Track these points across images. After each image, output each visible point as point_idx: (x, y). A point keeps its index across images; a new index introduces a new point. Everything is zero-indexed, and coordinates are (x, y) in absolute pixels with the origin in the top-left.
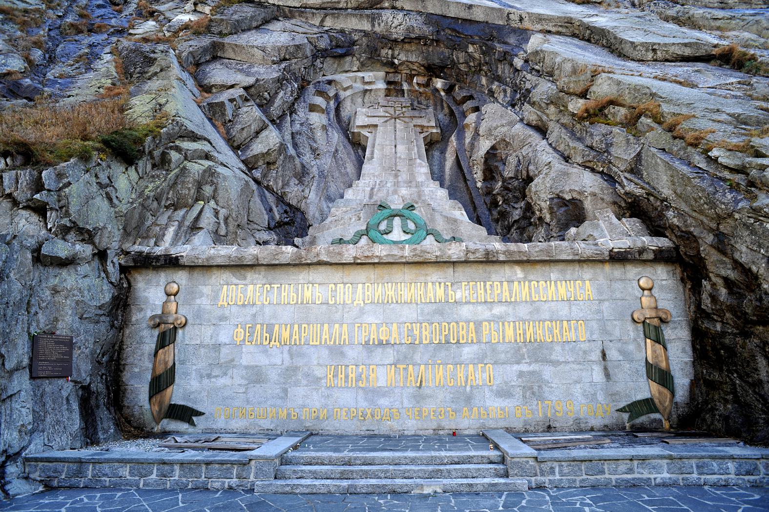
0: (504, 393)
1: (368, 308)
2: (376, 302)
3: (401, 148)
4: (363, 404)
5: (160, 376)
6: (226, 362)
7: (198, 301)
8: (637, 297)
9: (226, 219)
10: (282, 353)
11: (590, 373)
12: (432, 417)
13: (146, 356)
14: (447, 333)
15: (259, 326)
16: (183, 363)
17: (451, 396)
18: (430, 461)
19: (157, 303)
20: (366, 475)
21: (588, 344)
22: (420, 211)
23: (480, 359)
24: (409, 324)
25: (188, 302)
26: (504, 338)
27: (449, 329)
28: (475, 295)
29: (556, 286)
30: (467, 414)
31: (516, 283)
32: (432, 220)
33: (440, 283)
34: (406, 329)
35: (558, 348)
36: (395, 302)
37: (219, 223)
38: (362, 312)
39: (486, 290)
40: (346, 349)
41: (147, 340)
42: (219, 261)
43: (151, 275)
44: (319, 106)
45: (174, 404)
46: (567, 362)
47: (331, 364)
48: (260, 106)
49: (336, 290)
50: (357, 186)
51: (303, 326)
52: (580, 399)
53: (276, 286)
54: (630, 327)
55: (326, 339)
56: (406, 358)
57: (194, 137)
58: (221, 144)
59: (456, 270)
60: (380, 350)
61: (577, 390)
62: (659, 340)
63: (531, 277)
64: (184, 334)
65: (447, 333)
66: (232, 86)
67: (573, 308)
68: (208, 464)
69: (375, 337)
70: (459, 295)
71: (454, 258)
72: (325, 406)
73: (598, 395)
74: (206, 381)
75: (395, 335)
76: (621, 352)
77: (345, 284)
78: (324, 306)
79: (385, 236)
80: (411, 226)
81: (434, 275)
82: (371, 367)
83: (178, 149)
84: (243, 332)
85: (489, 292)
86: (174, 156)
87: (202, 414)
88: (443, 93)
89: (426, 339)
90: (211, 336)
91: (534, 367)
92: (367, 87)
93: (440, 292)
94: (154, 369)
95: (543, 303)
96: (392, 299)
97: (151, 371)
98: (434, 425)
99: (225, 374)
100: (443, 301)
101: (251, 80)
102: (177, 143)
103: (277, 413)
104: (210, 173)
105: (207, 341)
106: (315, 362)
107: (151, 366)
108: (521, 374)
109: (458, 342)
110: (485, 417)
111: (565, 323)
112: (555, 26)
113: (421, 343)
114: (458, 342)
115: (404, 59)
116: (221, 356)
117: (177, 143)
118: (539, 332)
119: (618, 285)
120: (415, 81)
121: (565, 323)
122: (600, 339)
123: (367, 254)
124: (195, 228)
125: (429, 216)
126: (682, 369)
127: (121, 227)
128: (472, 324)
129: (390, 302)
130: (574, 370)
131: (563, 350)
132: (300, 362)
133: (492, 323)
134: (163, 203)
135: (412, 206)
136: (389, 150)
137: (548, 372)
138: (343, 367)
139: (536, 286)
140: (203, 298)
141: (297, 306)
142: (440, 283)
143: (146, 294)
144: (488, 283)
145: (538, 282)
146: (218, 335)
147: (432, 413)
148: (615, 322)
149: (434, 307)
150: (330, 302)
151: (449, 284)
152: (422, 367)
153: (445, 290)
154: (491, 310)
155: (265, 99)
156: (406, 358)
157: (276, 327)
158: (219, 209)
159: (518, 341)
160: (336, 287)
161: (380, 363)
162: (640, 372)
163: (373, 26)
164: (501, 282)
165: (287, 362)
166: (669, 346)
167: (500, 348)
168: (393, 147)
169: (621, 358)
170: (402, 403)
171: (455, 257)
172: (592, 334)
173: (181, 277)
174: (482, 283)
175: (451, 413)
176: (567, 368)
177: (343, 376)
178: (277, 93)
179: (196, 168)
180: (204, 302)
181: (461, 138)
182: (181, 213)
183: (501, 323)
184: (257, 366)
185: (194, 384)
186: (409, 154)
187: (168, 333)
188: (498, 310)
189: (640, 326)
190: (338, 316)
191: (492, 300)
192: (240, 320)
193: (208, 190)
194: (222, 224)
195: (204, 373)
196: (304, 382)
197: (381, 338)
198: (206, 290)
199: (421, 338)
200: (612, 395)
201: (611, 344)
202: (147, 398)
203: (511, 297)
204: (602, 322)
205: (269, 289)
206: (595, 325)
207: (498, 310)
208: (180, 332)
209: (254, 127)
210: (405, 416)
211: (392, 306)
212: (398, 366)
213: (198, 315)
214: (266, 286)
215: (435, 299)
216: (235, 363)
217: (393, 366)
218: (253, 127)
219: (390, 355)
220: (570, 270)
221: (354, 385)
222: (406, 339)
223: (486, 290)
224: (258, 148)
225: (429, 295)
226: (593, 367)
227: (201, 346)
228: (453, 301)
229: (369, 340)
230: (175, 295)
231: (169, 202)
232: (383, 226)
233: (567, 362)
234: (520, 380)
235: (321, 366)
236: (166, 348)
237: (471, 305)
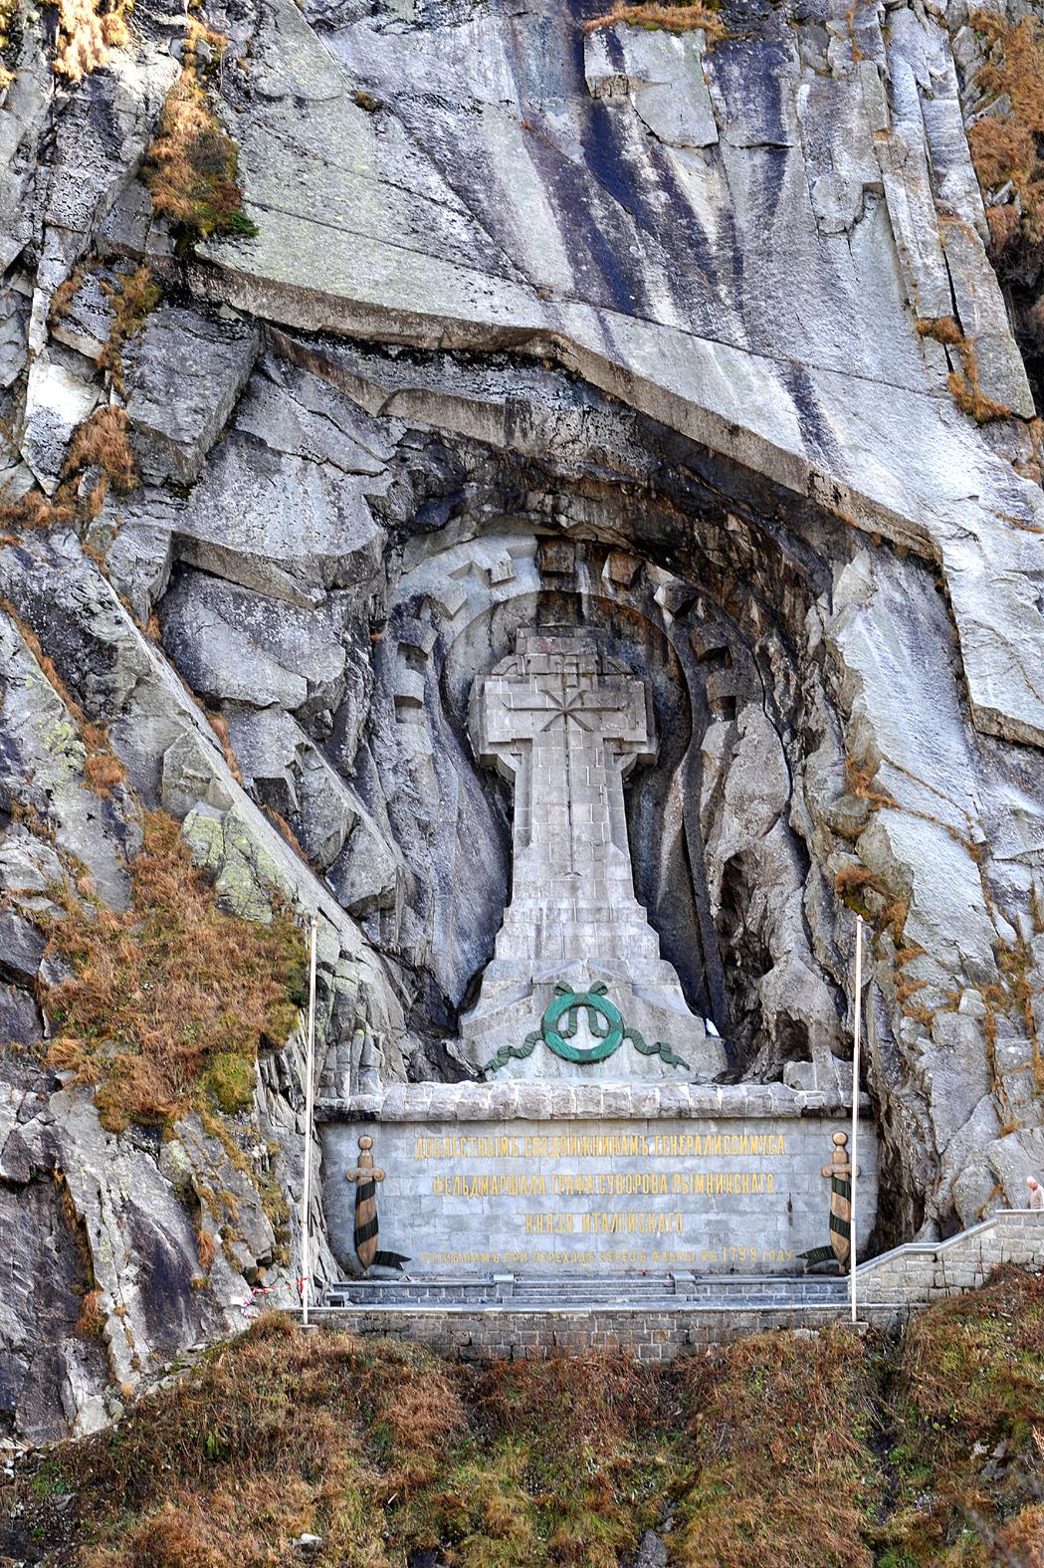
0: (692, 1239)
3: (580, 811)
4: (560, 1249)
7: (394, 1155)
16: (385, 1213)
18: (622, 1285)
20: (577, 1293)
22: (614, 996)
23: (671, 1209)
32: (632, 1012)
35: (746, 1200)
40: (543, 1199)
42: (417, 1118)
43: (341, 1129)
44: (413, 698)
46: (753, 1213)
50: (512, 922)
54: (819, 1181)
61: (761, 1238)
63: (725, 1132)
68: (465, 1287)
70: (652, 1148)
71: (648, 1116)
72: (525, 1251)
74: (409, 1229)
79: (567, 1041)
80: (602, 1023)
81: (629, 1130)
87: (408, 1260)
88: (668, 617)
91: (722, 1216)
92: (499, 595)
93: (634, 1146)
94: (356, 1220)
98: (626, 1267)
105: (407, 1192)
108: (709, 1223)
112: (900, 533)
115: (582, 517)
118: (730, 1186)
119: (812, 1140)
120: (606, 573)
132: (500, 1211)
135: (604, 987)
136: (558, 815)
137: (734, 1221)
163: (510, 433)
165: (487, 1212)
167: (691, 1198)
168: (566, 809)
172: (780, 1186)
173: (373, 1133)
176: (754, 1218)
180: (400, 1156)
181: (693, 782)
185: (398, 1233)
186: (595, 830)
188: (689, 1163)
189: (830, 1181)
190: (535, 1168)
196: (505, 1230)
198: (401, 1143)
204: (792, 1176)
206: (784, 1178)
207: (689, 1163)
213: (395, 1167)
219: (585, 1205)
220: (763, 1125)
227: (402, 1197)
232: (563, 1026)
233: (753, 1213)
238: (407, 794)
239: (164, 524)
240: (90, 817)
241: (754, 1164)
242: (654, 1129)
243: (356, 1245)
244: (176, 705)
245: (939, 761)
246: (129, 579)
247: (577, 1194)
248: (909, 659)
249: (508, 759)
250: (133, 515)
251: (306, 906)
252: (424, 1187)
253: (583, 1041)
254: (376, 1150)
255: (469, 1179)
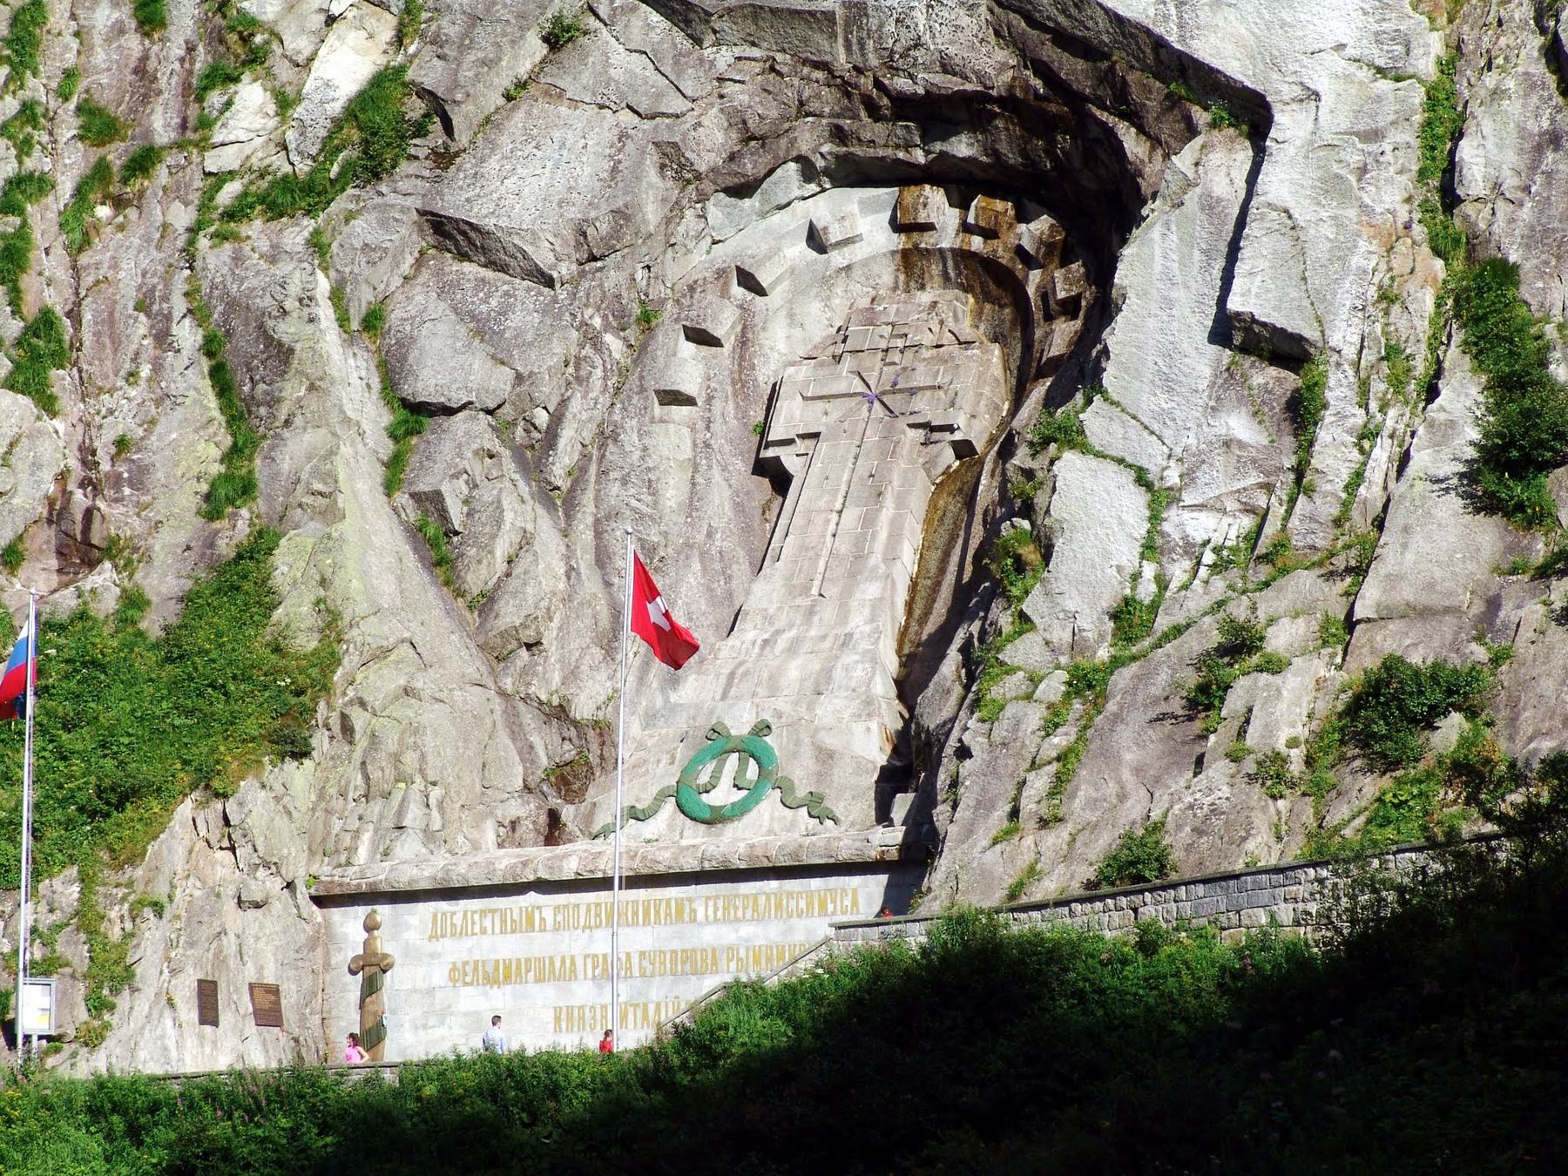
5: (370, 1029)
7: (405, 935)
9: (440, 804)
13: (352, 1005)
16: (394, 1012)
74: (421, 1032)
79: (704, 797)
99: (442, 1023)
105: (420, 985)
116: (436, 1001)
125: (791, 747)
127: (305, 847)
134: (350, 798)
135: (768, 727)
143: (344, 930)
193: (410, 759)
194: (435, 813)
195: (419, 1023)
227: (414, 991)
231: (358, 793)
238: (634, 510)
239: (409, 201)
240: (188, 548)
244: (342, 412)
245: (1170, 390)
246: (347, 270)
248: (1197, 265)
249: (790, 460)
250: (380, 194)
251: (366, 633)
253: (723, 795)
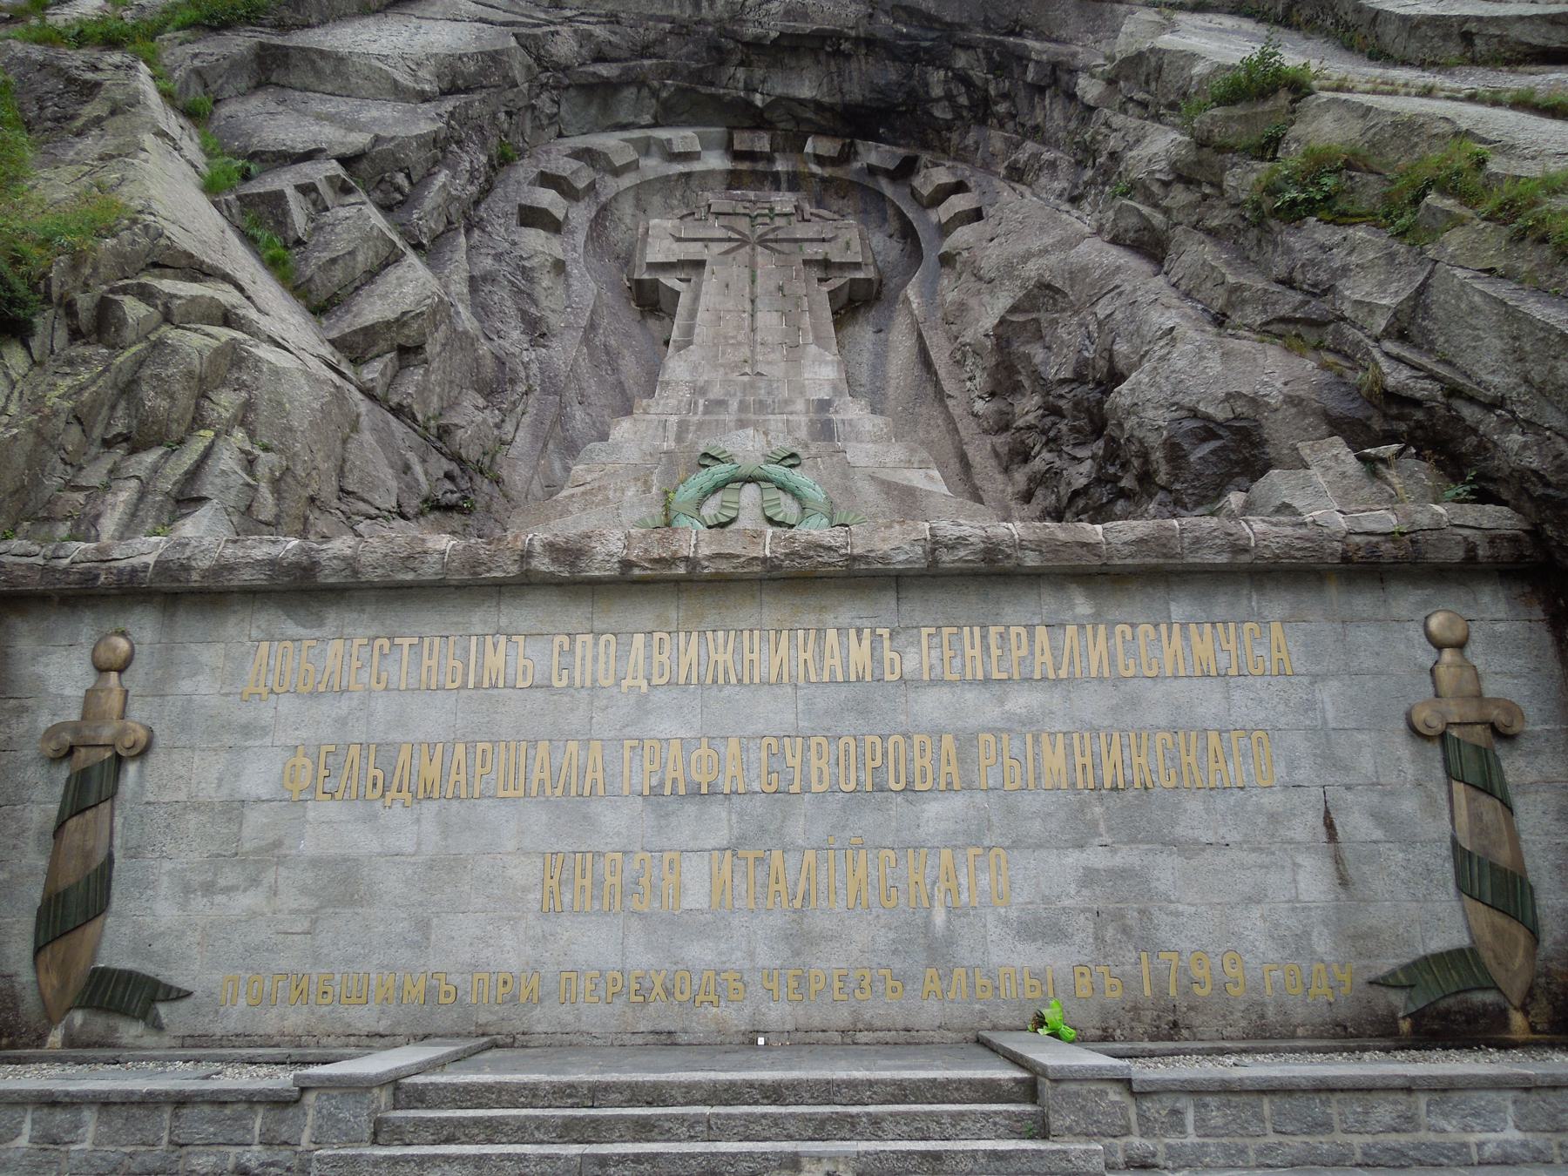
1: (659, 696)
2: (682, 681)
4: (642, 959)
5: (66, 892)
6: (256, 852)
7: (186, 686)
8: (1421, 668)
10: (418, 820)
11: (1288, 876)
12: (837, 996)
14: (878, 763)
15: (354, 750)
16: (135, 853)
17: (891, 935)
19: (67, 692)
21: (1280, 797)
23: (971, 836)
24: (773, 742)
25: (158, 691)
26: (1038, 778)
27: (885, 754)
28: (957, 662)
29: (1186, 637)
30: (936, 986)
31: (1071, 630)
33: (859, 631)
34: (764, 754)
35: (1194, 805)
36: (733, 680)
37: (255, 489)
38: (642, 705)
39: (986, 648)
41: (38, 795)
45: (105, 971)
47: (556, 848)
48: (386, 208)
49: (572, 651)
51: (480, 746)
52: (1262, 947)
53: (406, 642)
54: (1403, 748)
55: (541, 782)
56: (763, 829)
57: (198, 271)
58: (267, 290)
59: (902, 595)
60: (691, 809)
61: (1253, 924)
62: (1489, 785)
64: (141, 773)
65: (878, 763)
66: (309, 156)
67: (1237, 695)
69: (679, 774)
70: (911, 663)
73: (1314, 938)
74: (199, 902)
75: (732, 769)
76: (1379, 817)
77: (598, 634)
78: (539, 694)
82: (667, 856)
83: (145, 294)
84: (310, 766)
85: (995, 652)
86: (134, 309)
87: (185, 995)
89: (820, 781)
90: (220, 780)
91: (1127, 857)
93: (860, 653)
94: (52, 872)
95: (1149, 683)
96: (726, 672)
97: (42, 879)
99: (254, 882)
100: (868, 678)
101: (360, 140)
102: (145, 279)
103: (401, 988)
104: (234, 357)
105: (209, 791)
106: (511, 845)
107: (42, 863)
108: (1089, 877)
109: (909, 789)
110: (989, 994)
111: (1213, 737)
113: (806, 789)
114: (909, 789)
116: (247, 832)
117: (145, 279)
121: (1213, 737)
122: (1318, 782)
123: (656, 553)
124: (186, 499)
126: (1559, 867)
128: (948, 740)
129: (721, 681)
130: (1242, 867)
131: (1207, 811)
133: (1005, 736)
134: (97, 432)
137: (1166, 871)
138: (589, 856)
139: (1129, 637)
140: (200, 678)
141: (464, 693)
142: (859, 631)
143: (39, 669)
144: (993, 630)
145: (1133, 626)
146: (237, 776)
147: (837, 984)
148: (1360, 737)
149: (844, 692)
150: (556, 683)
151: (885, 632)
152: (810, 856)
153: (873, 649)
154: (1002, 702)
155: (399, 189)
156: (763, 829)
157: (404, 756)
158: (257, 452)
159: (1080, 785)
160: (573, 642)
161: (692, 845)
162: (1438, 875)
164: (1030, 628)
166: (1519, 803)
167: (1029, 803)
169: (1378, 834)
170: (751, 955)
171: (902, 557)
172: (1292, 766)
174: (977, 630)
175: (890, 983)
177: (587, 882)
178: (430, 175)
179: (196, 342)
182: (150, 457)
183: (1029, 738)
184: (345, 860)
185: (164, 911)
187: (95, 774)
188: (1021, 701)
189: (1435, 751)
191: (1004, 676)
192: (303, 733)
194: (265, 490)
195: (196, 879)
197: (697, 778)
198: (210, 655)
199: (806, 780)
200: (1355, 937)
201: (1350, 796)
202: (28, 953)
203: (1057, 669)
205: (386, 651)
207: (1021, 701)
208: (132, 769)
209: (363, 259)
210: (761, 992)
211: (727, 691)
212: (741, 853)
214: (378, 642)
215: (846, 672)
216: (284, 851)
217: (729, 853)
218: (360, 258)
219: (720, 825)
221: (618, 907)
222: (764, 779)
223: (986, 648)
224: (373, 309)
225: (828, 662)
226: (1300, 859)
228: (896, 677)
229: (662, 784)
230: (121, 671)
234: (1085, 892)
235: (527, 854)
236: (89, 814)
237: (946, 690)
241: (1209, 703)
242: (918, 610)
243: (38, 951)
247: (695, 793)
252: (257, 779)
254: (137, 676)
255: (385, 751)
